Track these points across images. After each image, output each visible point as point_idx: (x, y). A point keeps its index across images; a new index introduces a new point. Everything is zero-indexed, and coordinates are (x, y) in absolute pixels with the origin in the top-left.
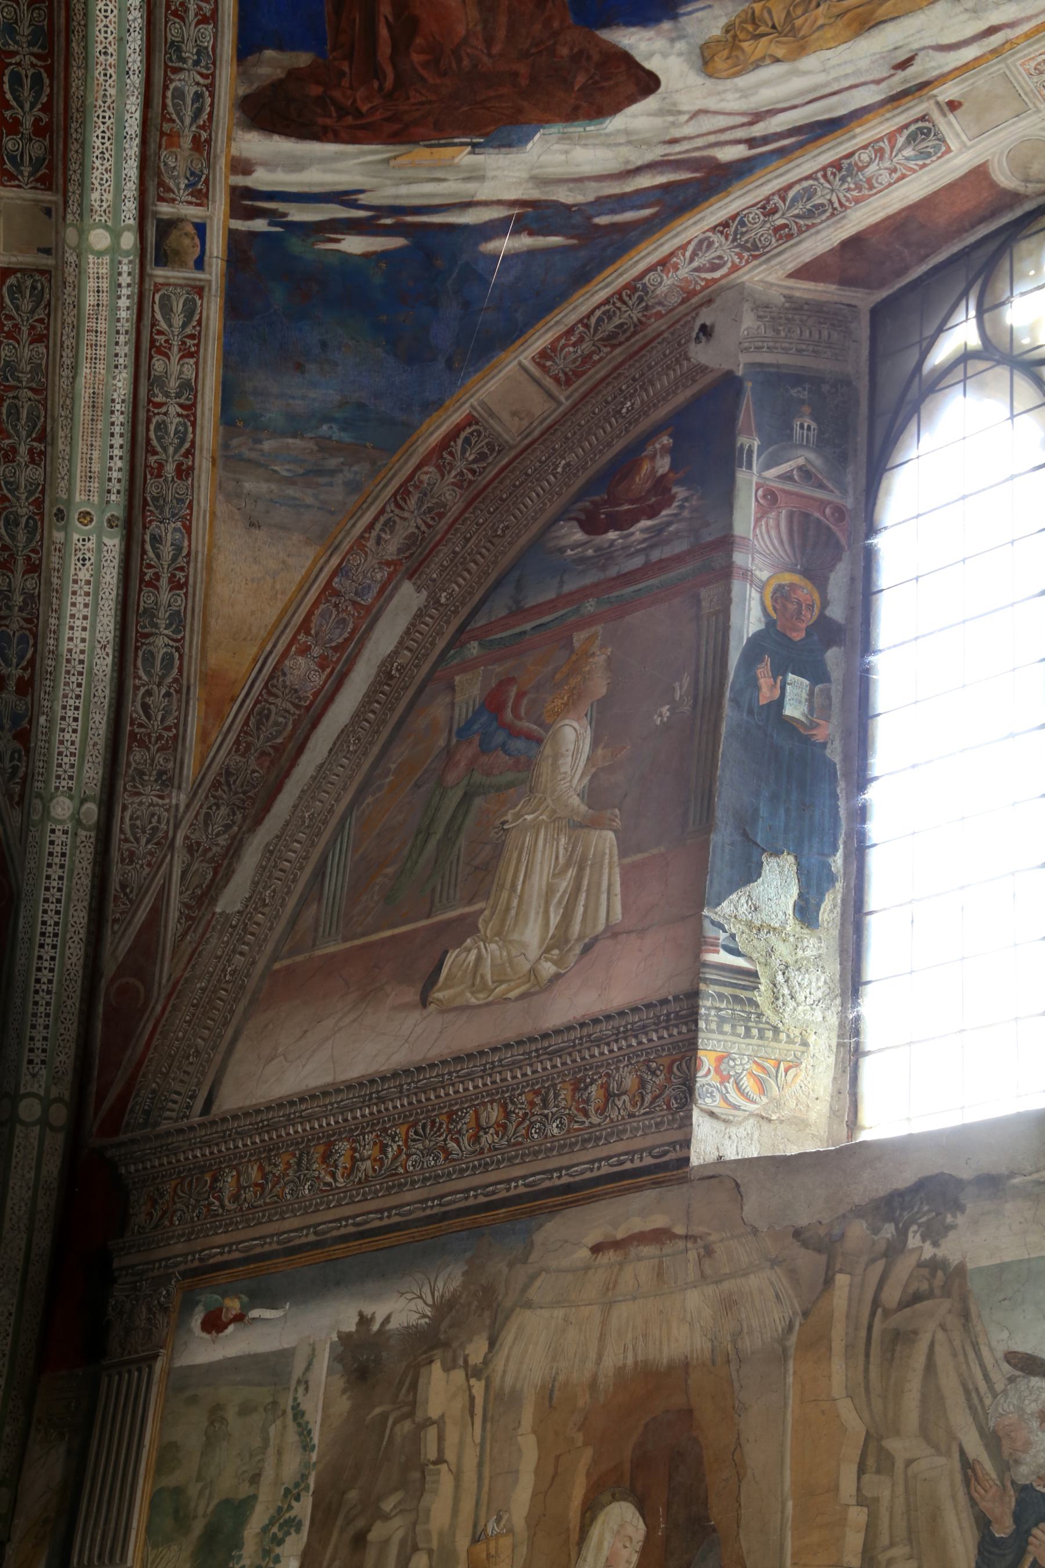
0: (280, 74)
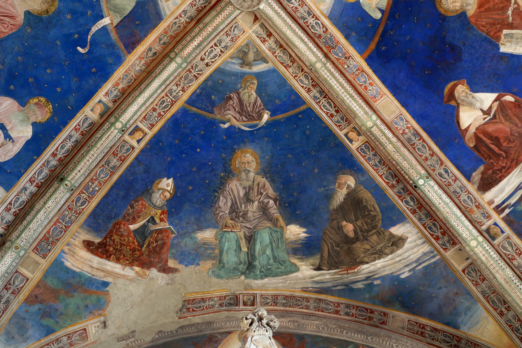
0: (480, 176)
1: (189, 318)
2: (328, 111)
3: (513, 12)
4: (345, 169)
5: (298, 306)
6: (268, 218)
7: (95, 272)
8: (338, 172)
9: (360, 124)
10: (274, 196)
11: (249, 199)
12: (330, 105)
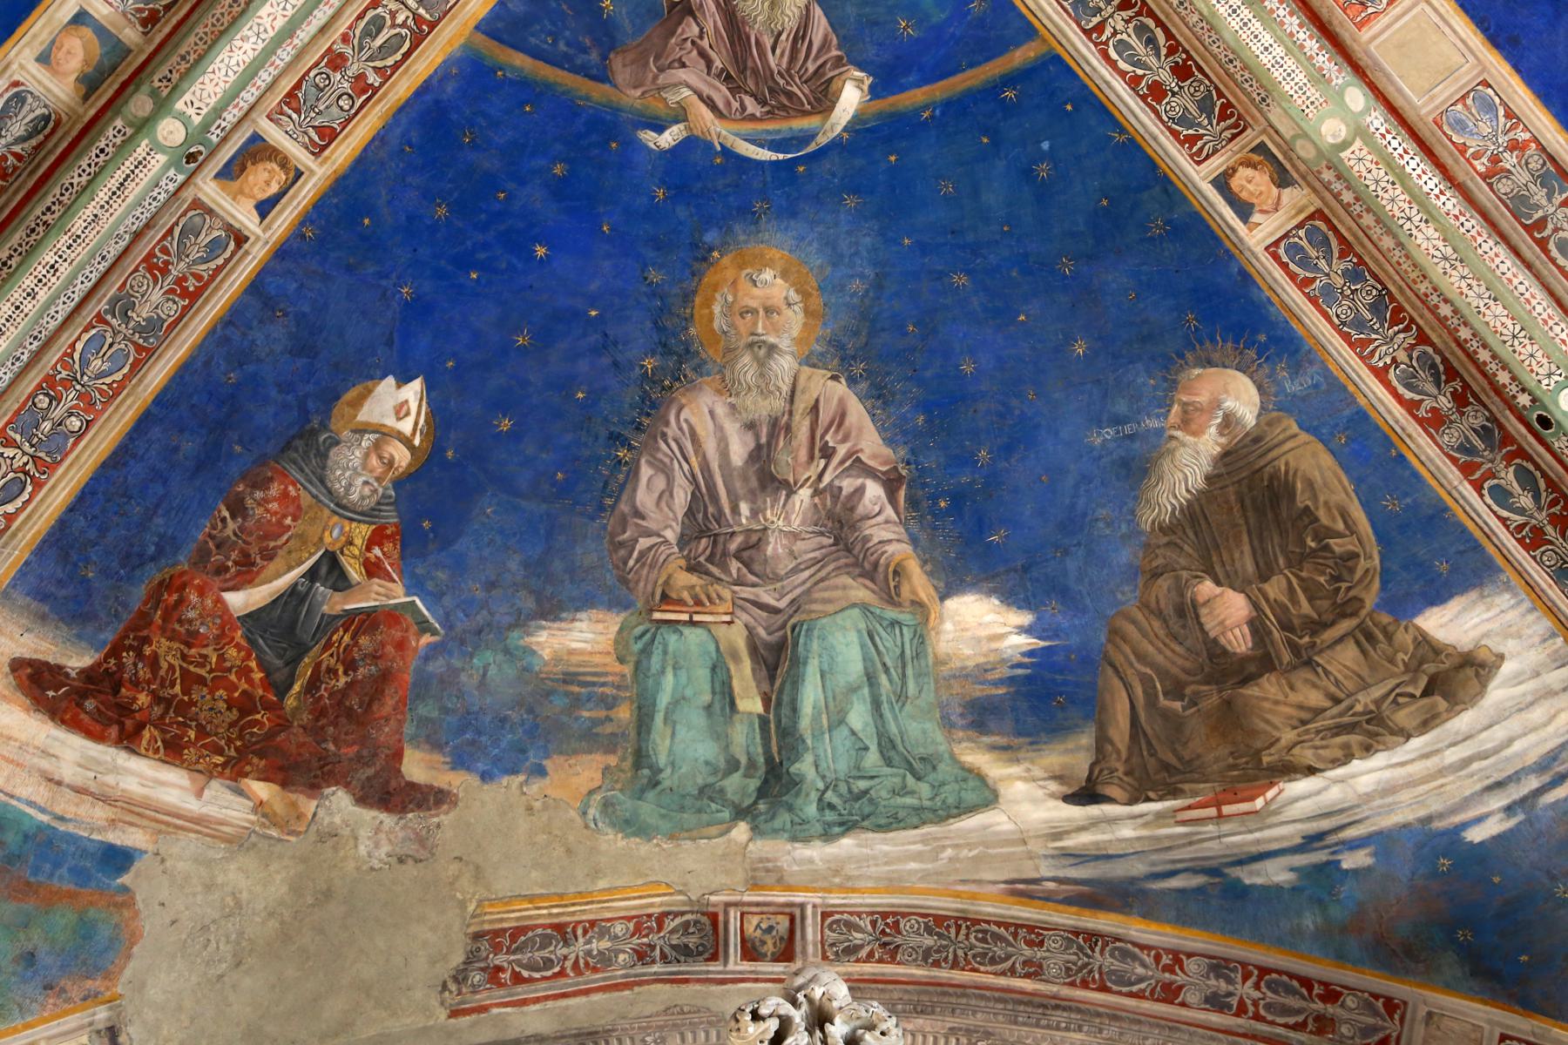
1: (495, 1011)
2: (1140, 72)
4: (1213, 340)
5: (993, 961)
6: (856, 565)
7: (67, 805)
8: (1182, 356)
9: (1286, 130)
10: (885, 463)
11: (773, 478)
12: (1151, 41)
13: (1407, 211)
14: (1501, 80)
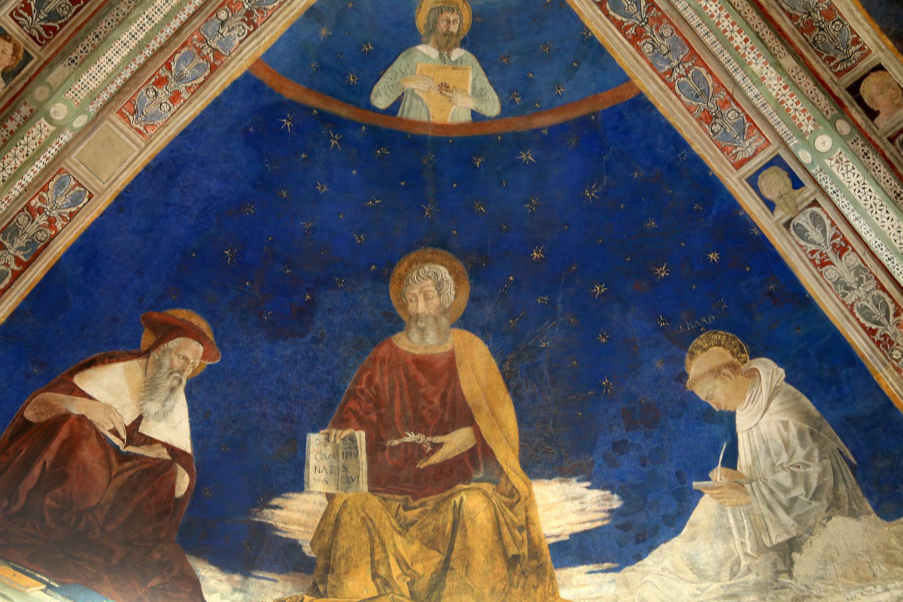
3: (413, 444)
13: (9, 167)
14: (94, 206)
